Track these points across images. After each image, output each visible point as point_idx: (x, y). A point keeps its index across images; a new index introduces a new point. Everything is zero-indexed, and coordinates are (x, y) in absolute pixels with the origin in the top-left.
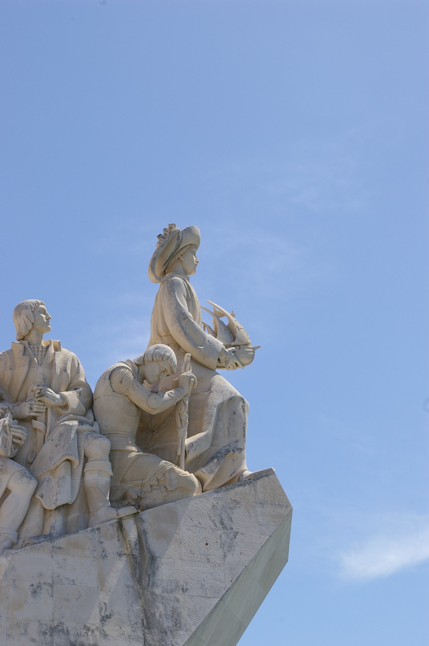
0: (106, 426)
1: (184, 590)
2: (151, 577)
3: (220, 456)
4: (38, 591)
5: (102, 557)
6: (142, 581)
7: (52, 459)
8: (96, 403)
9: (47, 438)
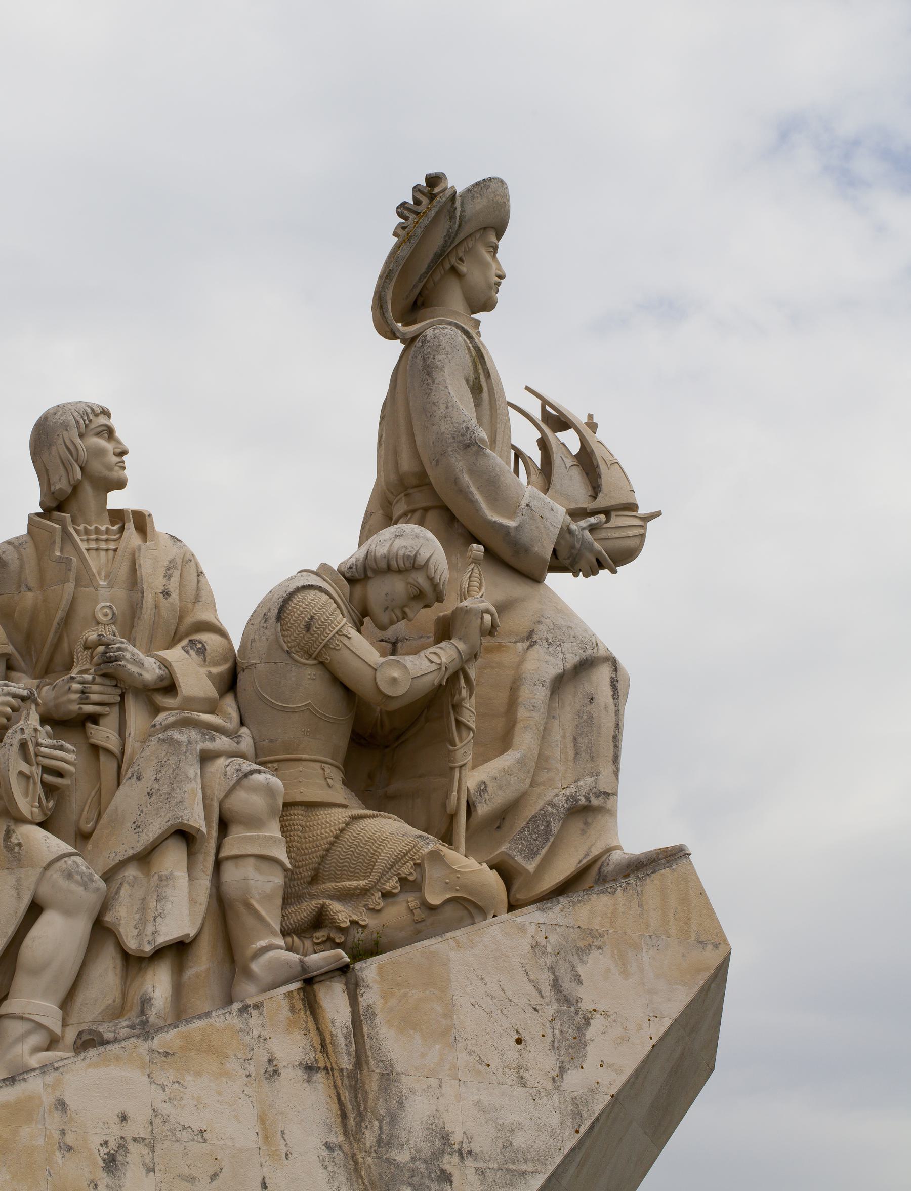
0: (271, 741)
1: (465, 1155)
2: (384, 1122)
3: (552, 813)
4: (119, 1158)
5: (267, 1075)
6: (364, 1134)
7: (139, 827)
8: (241, 677)
9: (127, 770)
